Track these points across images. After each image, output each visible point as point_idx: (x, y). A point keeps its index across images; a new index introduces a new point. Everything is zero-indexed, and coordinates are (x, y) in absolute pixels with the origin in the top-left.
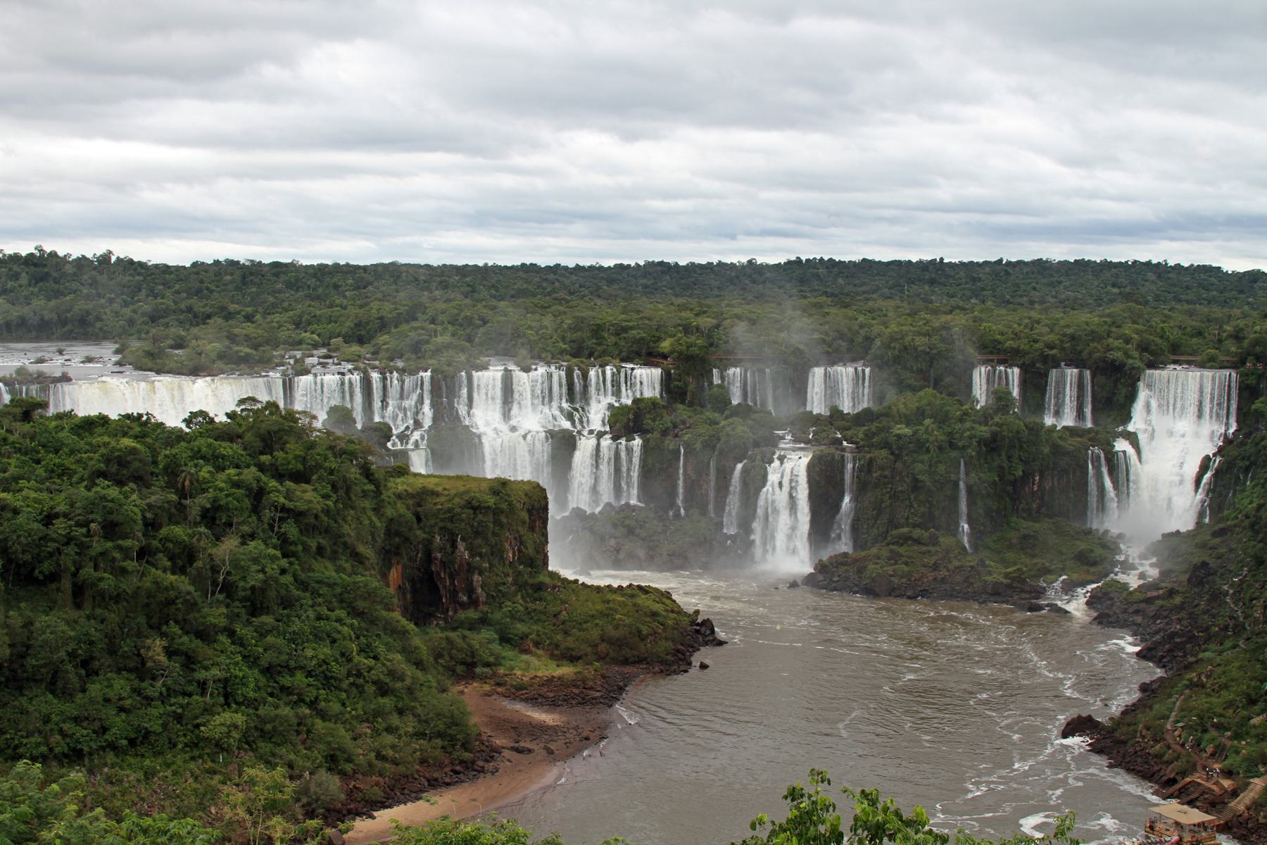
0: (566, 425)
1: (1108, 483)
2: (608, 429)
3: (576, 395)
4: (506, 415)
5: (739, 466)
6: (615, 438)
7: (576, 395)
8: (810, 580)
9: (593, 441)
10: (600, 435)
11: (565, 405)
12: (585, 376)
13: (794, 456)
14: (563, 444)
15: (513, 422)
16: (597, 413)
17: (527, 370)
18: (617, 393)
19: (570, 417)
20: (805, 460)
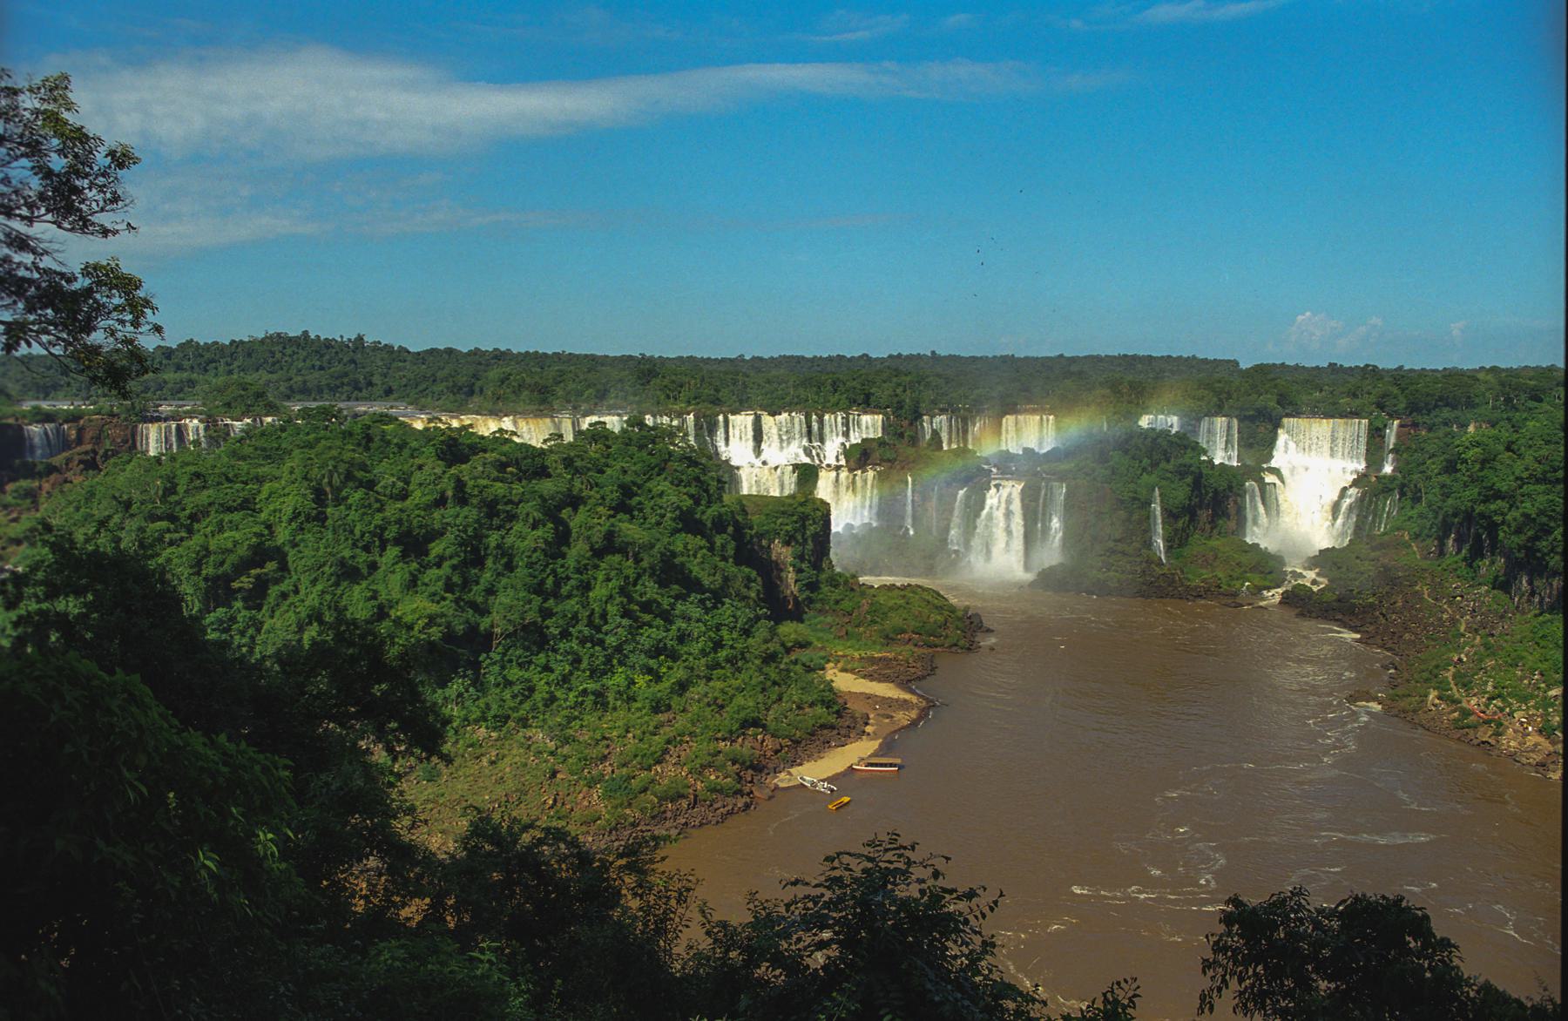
0: (807, 460)
1: (1261, 509)
2: (843, 462)
3: (814, 435)
4: (758, 450)
5: (961, 492)
6: (851, 470)
7: (814, 435)
8: (1032, 584)
9: (834, 474)
10: (838, 468)
11: (805, 442)
12: (821, 422)
13: (1011, 483)
14: (807, 474)
15: (763, 457)
16: (832, 448)
17: (773, 414)
18: (846, 434)
19: (807, 452)
20: (1019, 487)
